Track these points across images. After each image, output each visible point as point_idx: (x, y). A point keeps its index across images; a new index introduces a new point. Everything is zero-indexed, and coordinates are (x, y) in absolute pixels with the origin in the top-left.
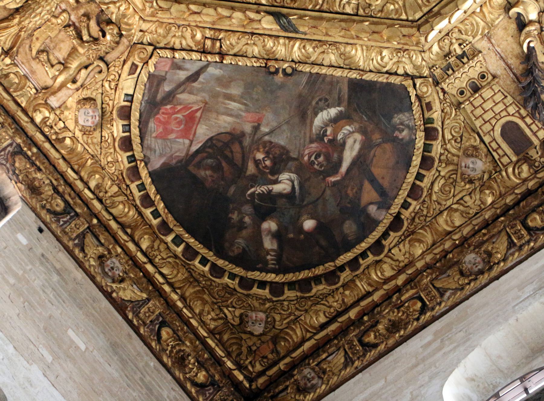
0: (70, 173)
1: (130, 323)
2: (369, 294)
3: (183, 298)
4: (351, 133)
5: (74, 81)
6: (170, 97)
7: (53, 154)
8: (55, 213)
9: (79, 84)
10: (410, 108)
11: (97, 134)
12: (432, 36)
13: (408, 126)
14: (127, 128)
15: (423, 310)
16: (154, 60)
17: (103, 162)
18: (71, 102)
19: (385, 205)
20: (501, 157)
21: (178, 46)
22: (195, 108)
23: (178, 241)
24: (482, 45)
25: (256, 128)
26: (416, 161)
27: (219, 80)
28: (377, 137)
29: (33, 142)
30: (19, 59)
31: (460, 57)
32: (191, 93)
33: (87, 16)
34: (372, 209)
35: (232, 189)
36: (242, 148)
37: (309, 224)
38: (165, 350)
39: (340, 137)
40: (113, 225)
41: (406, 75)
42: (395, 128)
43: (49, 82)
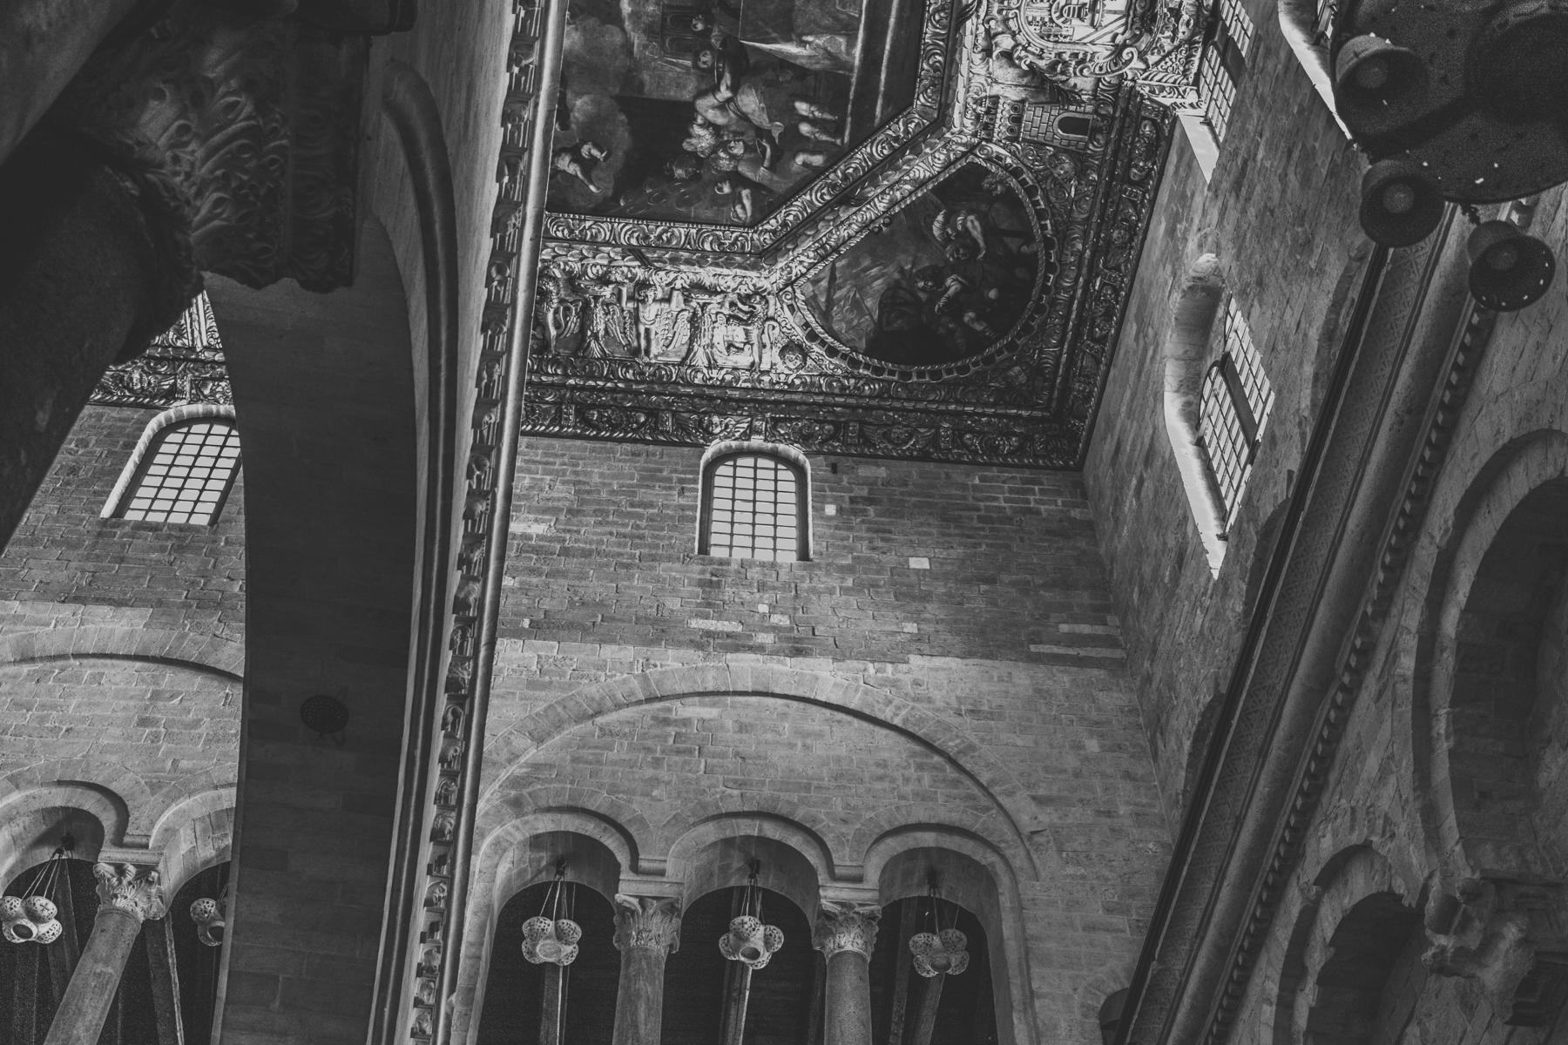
0: (820, 399)
1: (939, 461)
2: (1072, 298)
3: (957, 402)
4: (965, 220)
5: (764, 346)
6: (830, 302)
7: (796, 397)
8: (834, 437)
9: (768, 345)
10: (987, 171)
11: (809, 362)
12: (957, 121)
13: (997, 183)
14: (823, 343)
15: (1116, 291)
16: (798, 291)
17: (830, 372)
18: (778, 360)
19: (1028, 238)
20: (1076, 145)
21: (804, 270)
22: (852, 294)
23: (921, 375)
24: (996, 90)
25: (902, 271)
26: (1022, 195)
27: (849, 265)
28: (984, 207)
29: (776, 402)
30: (720, 362)
31: (987, 113)
32: (840, 288)
33: (732, 304)
34: (1025, 249)
35: (924, 318)
36: (904, 289)
37: (992, 294)
38: (976, 452)
39: (960, 228)
40: (874, 402)
41: (964, 155)
42: (989, 191)
43: (751, 359)
